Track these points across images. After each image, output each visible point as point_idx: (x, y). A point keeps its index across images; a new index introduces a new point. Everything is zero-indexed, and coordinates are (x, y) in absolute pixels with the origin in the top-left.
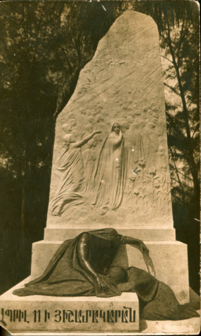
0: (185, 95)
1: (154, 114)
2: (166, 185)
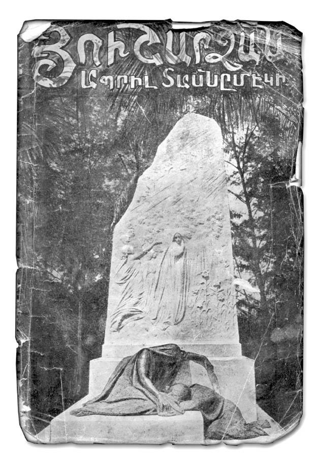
2: (231, 298)
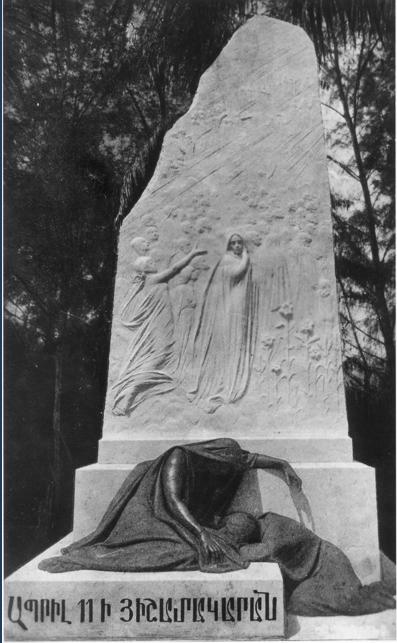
1: (309, 215)
2: (333, 353)
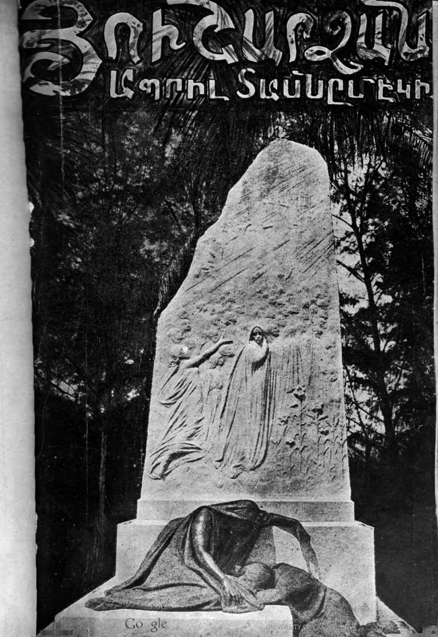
0: (372, 280)
1: (321, 311)
2: (339, 429)
